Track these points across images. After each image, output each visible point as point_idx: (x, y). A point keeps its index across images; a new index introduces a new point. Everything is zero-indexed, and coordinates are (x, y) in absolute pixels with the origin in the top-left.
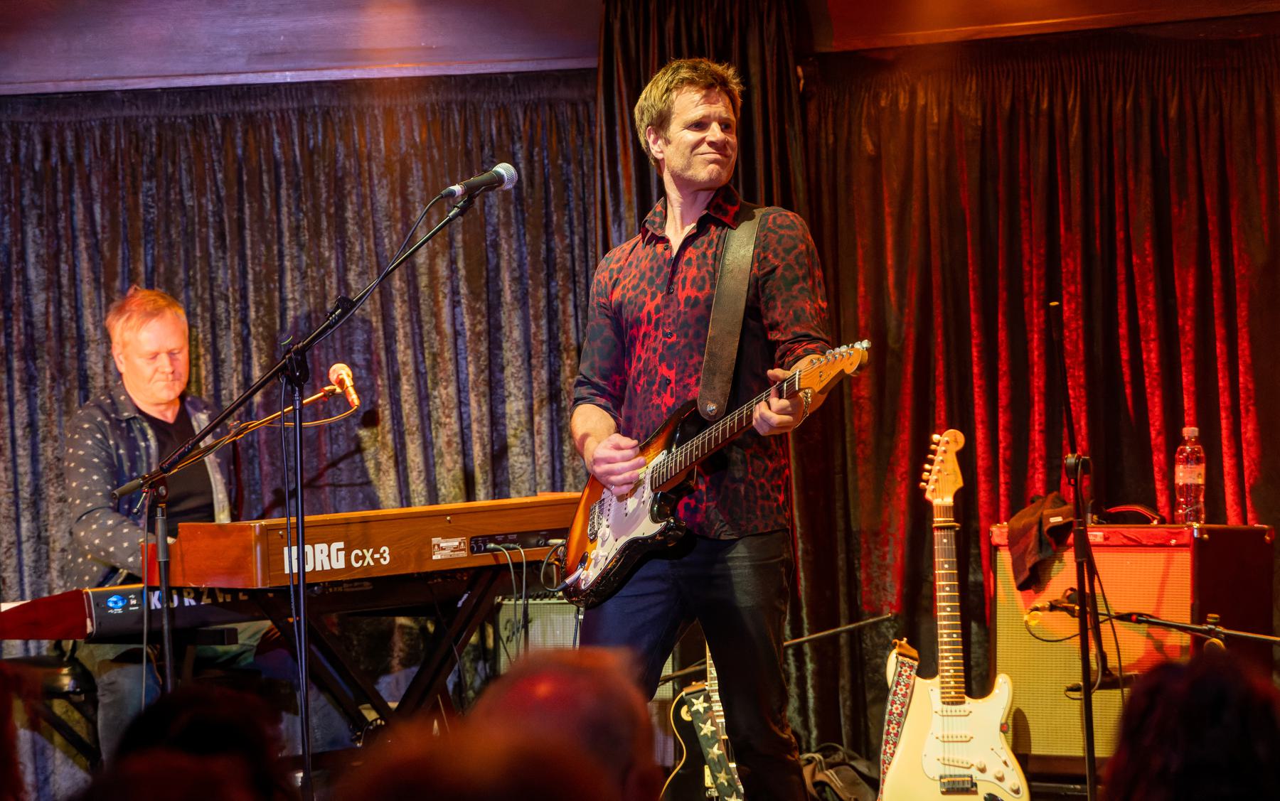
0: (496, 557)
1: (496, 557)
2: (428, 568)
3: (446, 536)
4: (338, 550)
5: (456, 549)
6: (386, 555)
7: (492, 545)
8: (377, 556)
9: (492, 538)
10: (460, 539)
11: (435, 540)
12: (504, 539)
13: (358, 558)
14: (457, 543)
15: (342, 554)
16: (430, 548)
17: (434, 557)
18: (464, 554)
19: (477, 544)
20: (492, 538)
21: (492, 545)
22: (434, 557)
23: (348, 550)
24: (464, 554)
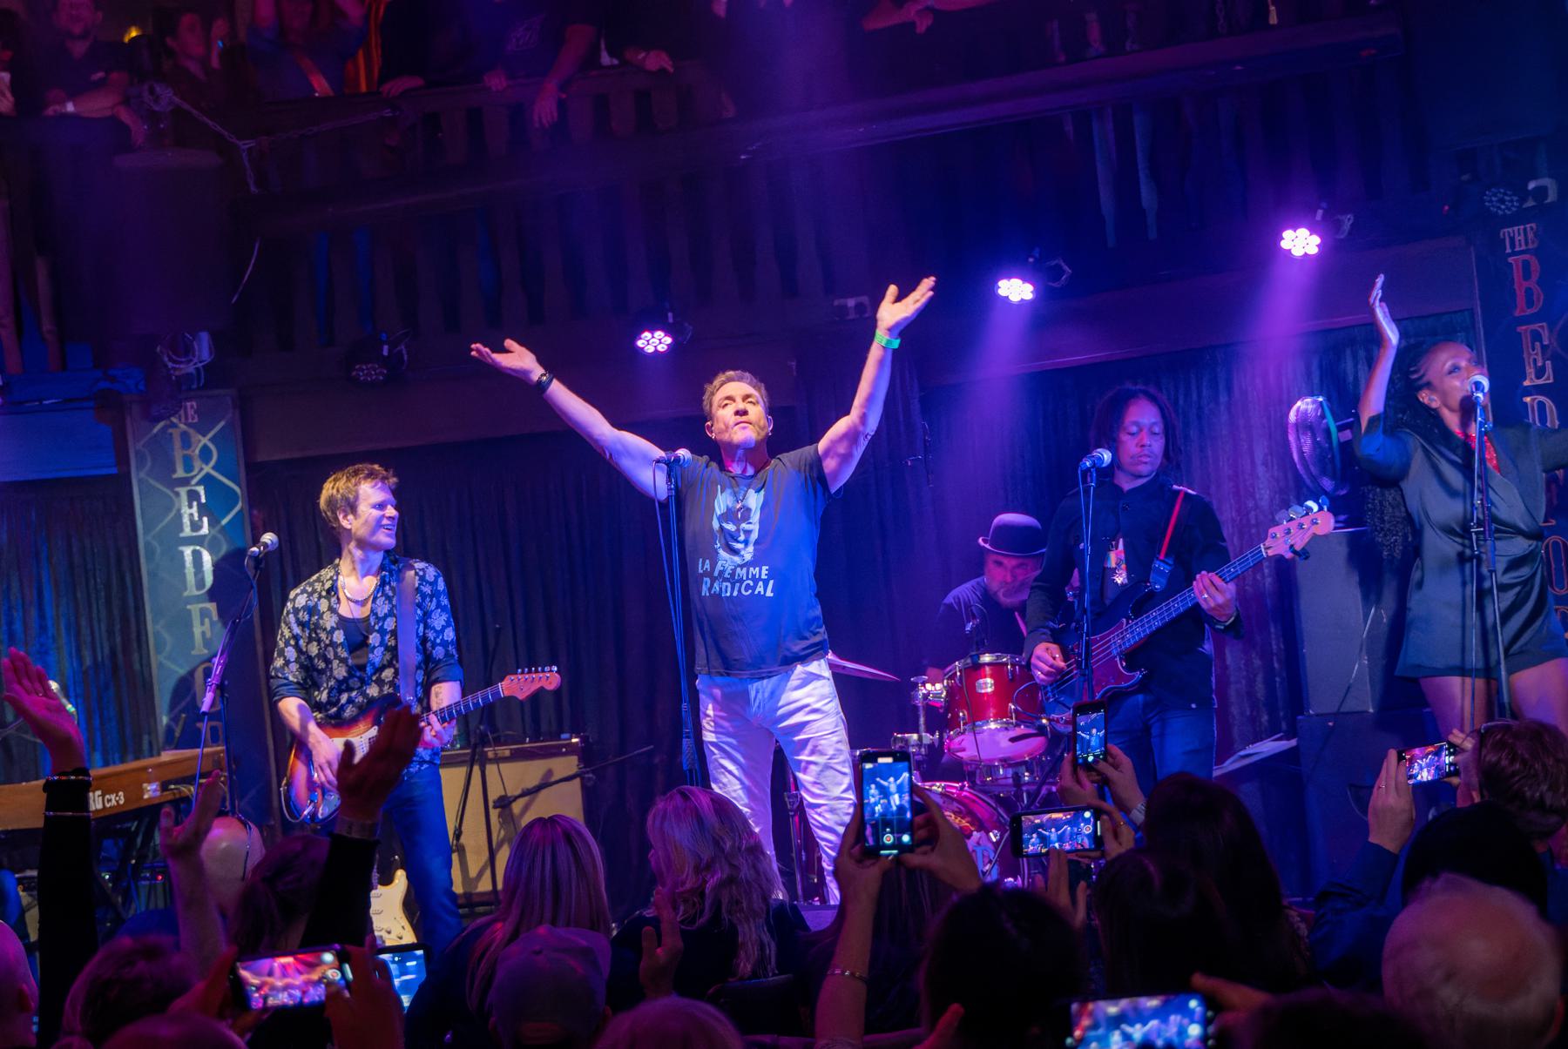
0: (174, 794)
1: (174, 794)
2: (143, 804)
3: (149, 782)
4: (99, 796)
5: (155, 791)
6: (122, 798)
7: (173, 787)
8: (117, 798)
9: (170, 782)
10: (157, 783)
11: (145, 785)
12: (176, 782)
13: (109, 801)
14: (154, 787)
15: (101, 798)
16: (142, 792)
17: (146, 797)
18: (158, 793)
19: (164, 787)
20: (170, 782)
21: (173, 787)
22: (146, 797)
23: (103, 795)
24: (158, 793)
